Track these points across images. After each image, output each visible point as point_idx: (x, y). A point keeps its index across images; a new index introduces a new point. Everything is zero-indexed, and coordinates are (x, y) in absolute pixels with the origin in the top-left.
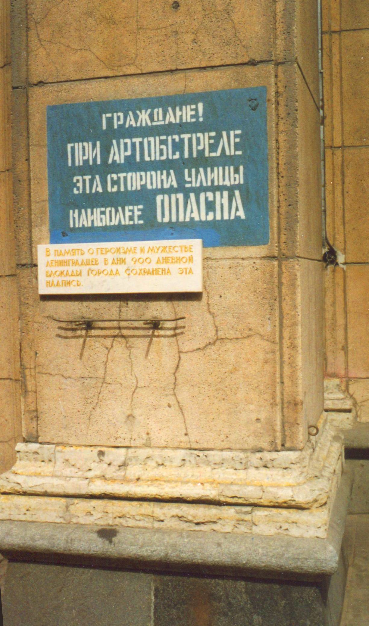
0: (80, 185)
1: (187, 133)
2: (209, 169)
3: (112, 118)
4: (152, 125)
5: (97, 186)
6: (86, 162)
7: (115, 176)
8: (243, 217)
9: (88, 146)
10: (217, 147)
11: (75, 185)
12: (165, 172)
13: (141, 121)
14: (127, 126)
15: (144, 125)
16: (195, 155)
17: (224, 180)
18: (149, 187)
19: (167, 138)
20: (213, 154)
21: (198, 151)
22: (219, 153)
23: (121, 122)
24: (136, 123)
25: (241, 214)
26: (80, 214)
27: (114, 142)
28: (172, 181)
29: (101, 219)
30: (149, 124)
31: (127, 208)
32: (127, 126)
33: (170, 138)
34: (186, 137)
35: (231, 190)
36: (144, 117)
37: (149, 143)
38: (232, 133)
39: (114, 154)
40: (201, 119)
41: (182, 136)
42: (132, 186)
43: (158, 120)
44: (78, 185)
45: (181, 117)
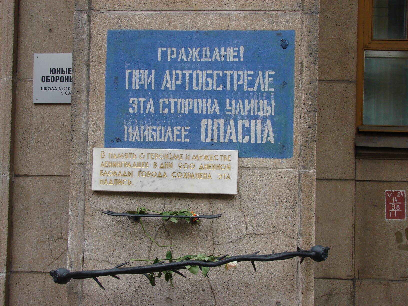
0: (135, 106)
1: (230, 69)
2: (247, 101)
3: (167, 51)
6: (142, 86)
7: (166, 100)
8: (272, 142)
12: (210, 101)
14: (179, 60)
15: (194, 60)
16: (235, 89)
18: (196, 112)
19: (213, 72)
20: (250, 89)
21: (238, 86)
22: (255, 89)
23: (174, 56)
24: (187, 57)
26: (134, 129)
27: (168, 72)
28: (215, 108)
29: (153, 136)
32: (179, 60)
34: (228, 73)
35: (264, 119)
36: (194, 52)
37: (197, 75)
38: (267, 73)
40: (242, 60)
41: (225, 72)
42: (181, 109)
44: (134, 105)
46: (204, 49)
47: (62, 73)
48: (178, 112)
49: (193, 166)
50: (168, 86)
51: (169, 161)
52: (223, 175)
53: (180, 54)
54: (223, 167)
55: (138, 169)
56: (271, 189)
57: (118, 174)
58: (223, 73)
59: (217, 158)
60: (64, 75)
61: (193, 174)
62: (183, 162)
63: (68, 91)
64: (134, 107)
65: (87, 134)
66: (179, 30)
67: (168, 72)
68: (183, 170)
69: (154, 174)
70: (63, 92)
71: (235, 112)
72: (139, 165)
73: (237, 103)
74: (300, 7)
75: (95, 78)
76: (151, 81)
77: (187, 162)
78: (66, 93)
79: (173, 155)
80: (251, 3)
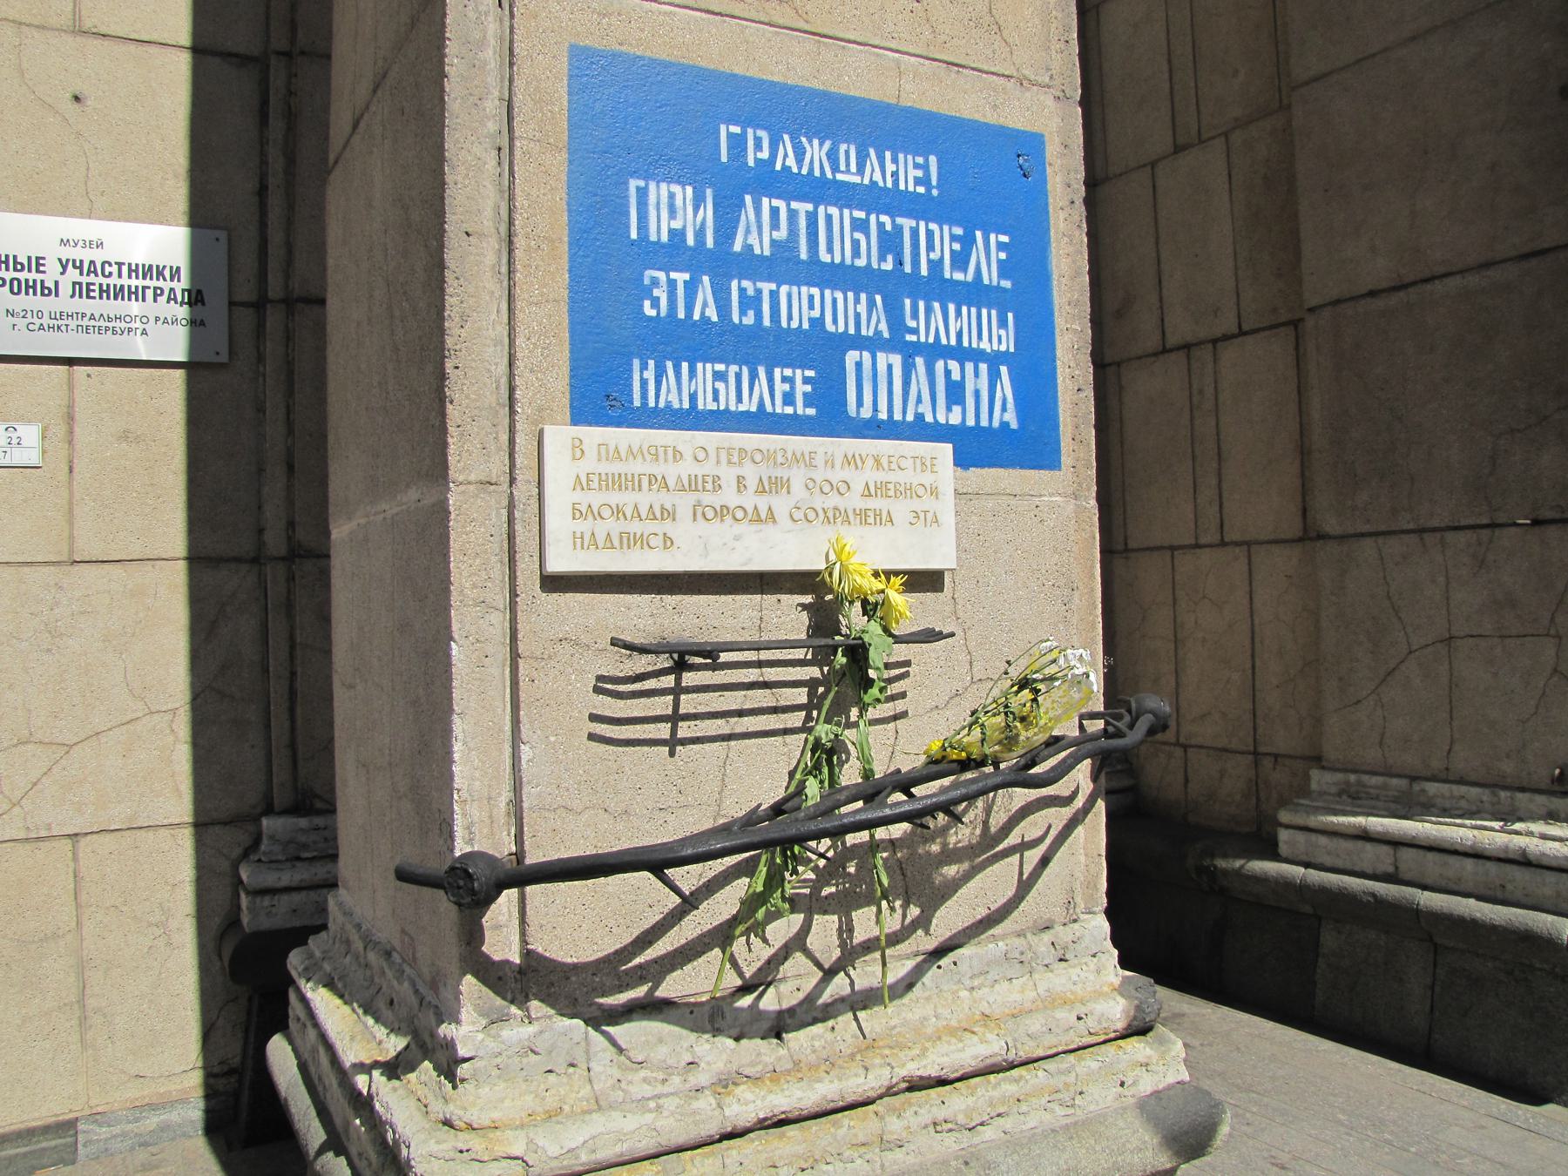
0: (661, 293)
2: (952, 308)
3: (744, 135)
4: (835, 181)
6: (677, 235)
10: (967, 262)
11: (647, 292)
12: (863, 296)
14: (778, 167)
15: (817, 173)
16: (924, 272)
18: (830, 327)
21: (929, 261)
24: (800, 162)
25: (1011, 418)
26: (660, 374)
27: (748, 198)
29: (716, 392)
32: (778, 167)
33: (873, 217)
34: (907, 223)
35: (994, 360)
36: (816, 152)
37: (829, 218)
39: (748, 231)
40: (935, 192)
42: (790, 318)
43: (848, 171)
44: (656, 292)
45: (895, 174)
46: (843, 147)
47: (15, 269)
48: (784, 324)
51: (779, 472)
52: (922, 515)
55: (692, 498)
57: (629, 516)
58: (893, 222)
60: (23, 276)
63: (38, 322)
64: (658, 298)
66: (776, 79)
70: (22, 323)
72: (693, 485)
73: (929, 311)
75: (534, 192)
76: (704, 219)
78: (31, 327)
79: (789, 455)
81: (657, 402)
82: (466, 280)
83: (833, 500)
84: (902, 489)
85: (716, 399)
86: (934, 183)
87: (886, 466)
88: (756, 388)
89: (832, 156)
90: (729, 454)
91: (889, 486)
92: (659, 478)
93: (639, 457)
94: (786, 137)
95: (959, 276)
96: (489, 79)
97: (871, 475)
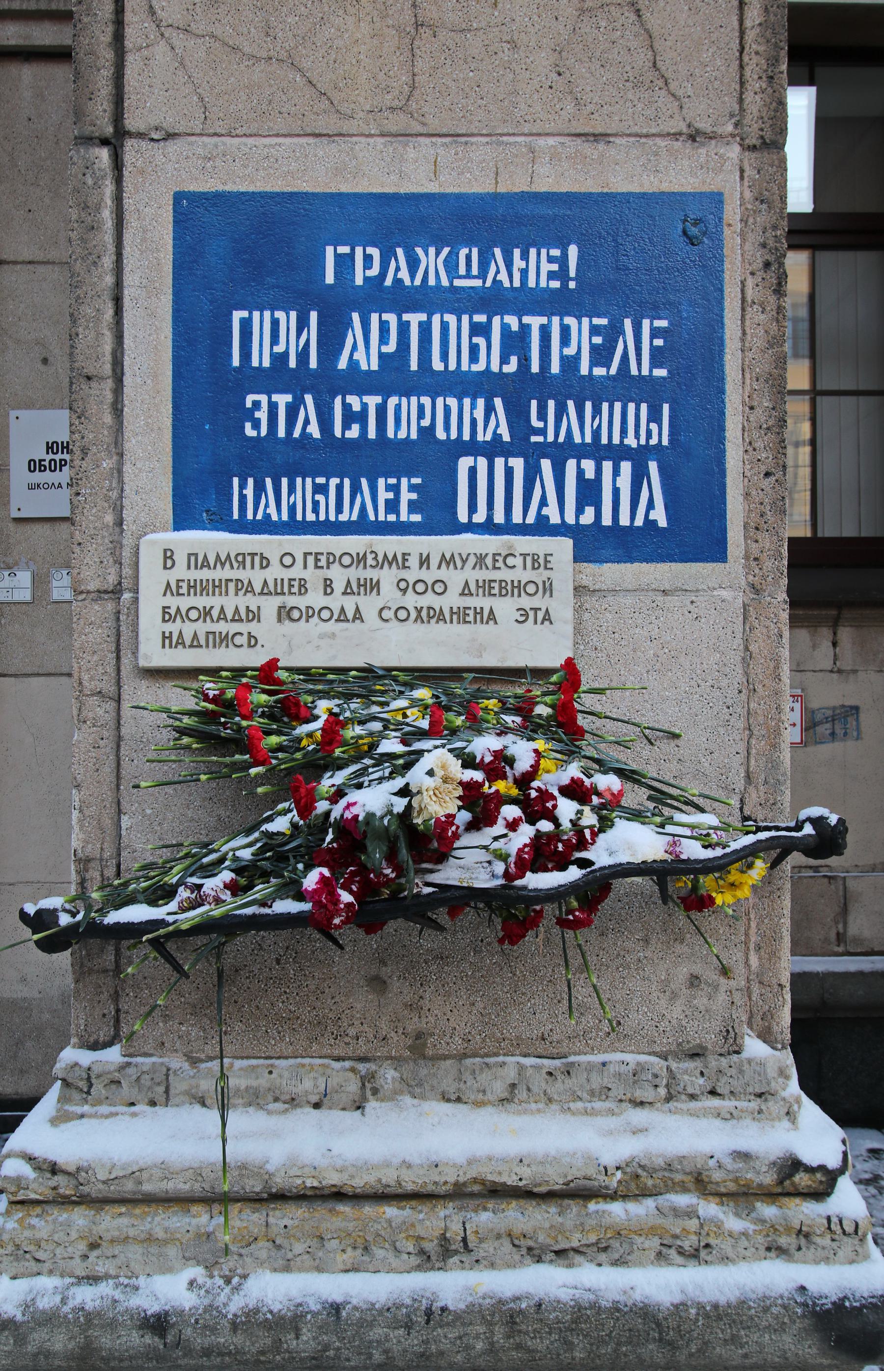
0: (262, 415)
3: (352, 255)
4: (453, 289)
5: (307, 422)
7: (354, 402)
9: (288, 320)
11: (249, 415)
12: (481, 402)
13: (426, 272)
14: (388, 282)
16: (555, 368)
17: (624, 432)
18: (441, 434)
21: (562, 358)
24: (412, 275)
26: (260, 489)
27: (356, 316)
28: (497, 426)
29: (316, 504)
30: (445, 282)
31: (381, 482)
32: (388, 282)
33: (496, 320)
34: (535, 322)
37: (445, 327)
38: (646, 323)
39: (354, 347)
40: (572, 285)
41: (526, 320)
44: (257, 415)
45: (524, 272)
46: (464, 252)
49: (440, 587)
50: (356, 356)
52: (531, 614)
53: (393, 264)
54: (531, 589)
55: (278, 601)
56: (667, 651)
57: (215, 619)
59: (510, 561)
61: (441, 609)
62: (411, 576)
65: (118, 503)
67: (356, 316)
68: (411, 600)
69: (325, 614)
71: (557, 435)
74: (736, 125)
76: (308, 341)
77: (424, 574)
80: (596, 114)
81: (255, 514)
82: (86, 418)
83: (429, 599)
84: (509, 588)
85: (316, 510)
86: (572, 273)
87: (490, 566)
88: (358, 500)
89: (451, 266)
90: (317, 560)
91: (492, 585)
92: (246, 582)
93: (227, 565)
94: (400, 251)
95: (599, 371)
96: (106, 237)
97: (473, 575)
